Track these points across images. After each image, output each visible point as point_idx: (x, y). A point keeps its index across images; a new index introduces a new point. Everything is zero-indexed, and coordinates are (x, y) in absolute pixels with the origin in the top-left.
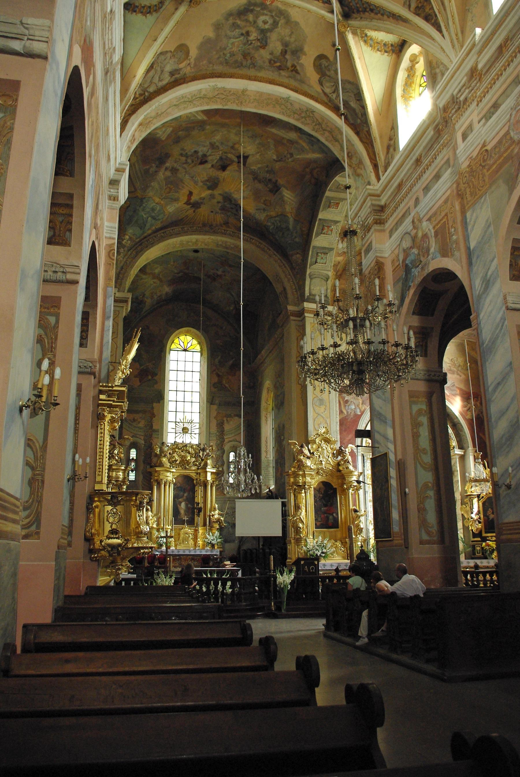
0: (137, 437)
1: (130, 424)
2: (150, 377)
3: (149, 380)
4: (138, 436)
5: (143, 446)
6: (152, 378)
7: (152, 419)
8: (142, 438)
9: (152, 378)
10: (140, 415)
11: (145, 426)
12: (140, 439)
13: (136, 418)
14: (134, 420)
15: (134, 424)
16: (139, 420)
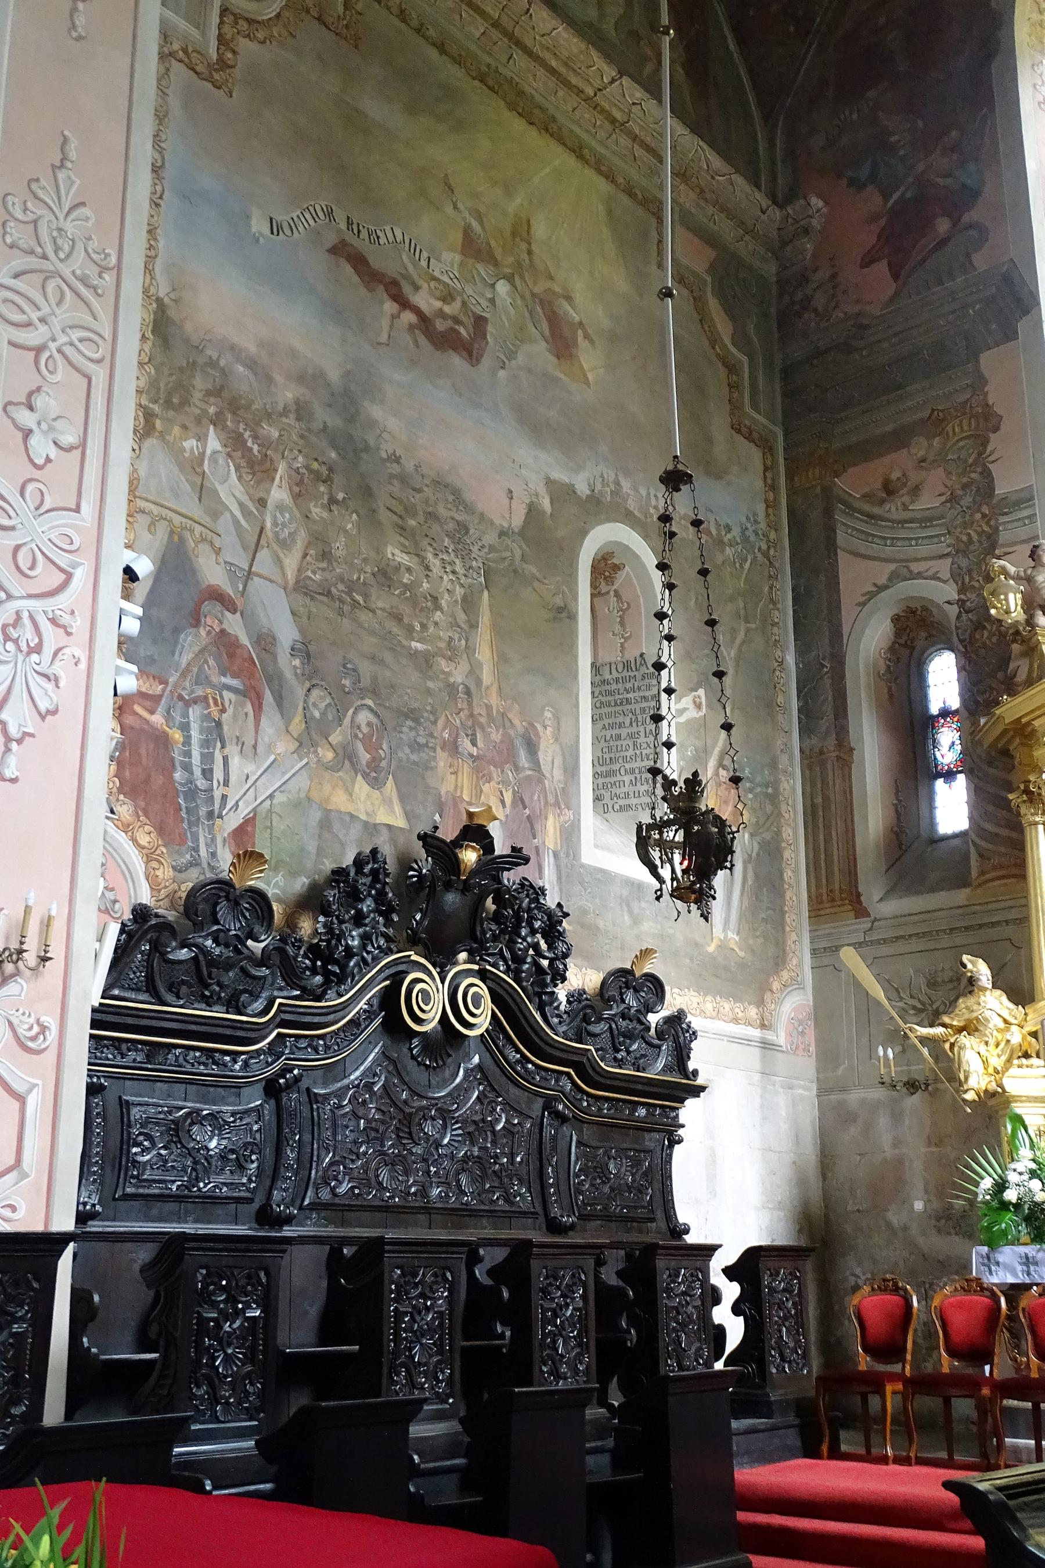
0: (919, 576)
1: (871, 516)
2: (943, 226)
3: (943, 242)
4: (915, 567)
5: (953, 610)
6: (956, 222)
7: (985, 443)
8: (944, 567)
9: (956, 222)
10: (920, 447)
11: (953, 499)
12: (935, 577)
13: (895, 475)
14: (890, 489)
15: (892, 509)
16: (914, 478)
